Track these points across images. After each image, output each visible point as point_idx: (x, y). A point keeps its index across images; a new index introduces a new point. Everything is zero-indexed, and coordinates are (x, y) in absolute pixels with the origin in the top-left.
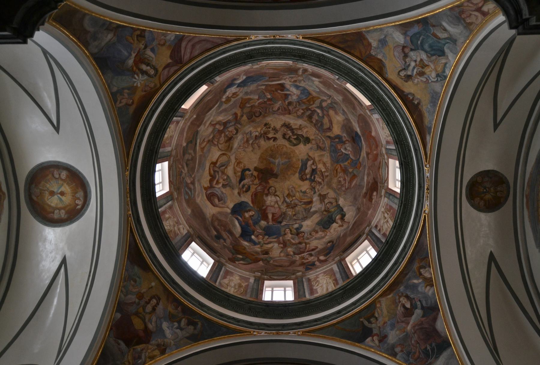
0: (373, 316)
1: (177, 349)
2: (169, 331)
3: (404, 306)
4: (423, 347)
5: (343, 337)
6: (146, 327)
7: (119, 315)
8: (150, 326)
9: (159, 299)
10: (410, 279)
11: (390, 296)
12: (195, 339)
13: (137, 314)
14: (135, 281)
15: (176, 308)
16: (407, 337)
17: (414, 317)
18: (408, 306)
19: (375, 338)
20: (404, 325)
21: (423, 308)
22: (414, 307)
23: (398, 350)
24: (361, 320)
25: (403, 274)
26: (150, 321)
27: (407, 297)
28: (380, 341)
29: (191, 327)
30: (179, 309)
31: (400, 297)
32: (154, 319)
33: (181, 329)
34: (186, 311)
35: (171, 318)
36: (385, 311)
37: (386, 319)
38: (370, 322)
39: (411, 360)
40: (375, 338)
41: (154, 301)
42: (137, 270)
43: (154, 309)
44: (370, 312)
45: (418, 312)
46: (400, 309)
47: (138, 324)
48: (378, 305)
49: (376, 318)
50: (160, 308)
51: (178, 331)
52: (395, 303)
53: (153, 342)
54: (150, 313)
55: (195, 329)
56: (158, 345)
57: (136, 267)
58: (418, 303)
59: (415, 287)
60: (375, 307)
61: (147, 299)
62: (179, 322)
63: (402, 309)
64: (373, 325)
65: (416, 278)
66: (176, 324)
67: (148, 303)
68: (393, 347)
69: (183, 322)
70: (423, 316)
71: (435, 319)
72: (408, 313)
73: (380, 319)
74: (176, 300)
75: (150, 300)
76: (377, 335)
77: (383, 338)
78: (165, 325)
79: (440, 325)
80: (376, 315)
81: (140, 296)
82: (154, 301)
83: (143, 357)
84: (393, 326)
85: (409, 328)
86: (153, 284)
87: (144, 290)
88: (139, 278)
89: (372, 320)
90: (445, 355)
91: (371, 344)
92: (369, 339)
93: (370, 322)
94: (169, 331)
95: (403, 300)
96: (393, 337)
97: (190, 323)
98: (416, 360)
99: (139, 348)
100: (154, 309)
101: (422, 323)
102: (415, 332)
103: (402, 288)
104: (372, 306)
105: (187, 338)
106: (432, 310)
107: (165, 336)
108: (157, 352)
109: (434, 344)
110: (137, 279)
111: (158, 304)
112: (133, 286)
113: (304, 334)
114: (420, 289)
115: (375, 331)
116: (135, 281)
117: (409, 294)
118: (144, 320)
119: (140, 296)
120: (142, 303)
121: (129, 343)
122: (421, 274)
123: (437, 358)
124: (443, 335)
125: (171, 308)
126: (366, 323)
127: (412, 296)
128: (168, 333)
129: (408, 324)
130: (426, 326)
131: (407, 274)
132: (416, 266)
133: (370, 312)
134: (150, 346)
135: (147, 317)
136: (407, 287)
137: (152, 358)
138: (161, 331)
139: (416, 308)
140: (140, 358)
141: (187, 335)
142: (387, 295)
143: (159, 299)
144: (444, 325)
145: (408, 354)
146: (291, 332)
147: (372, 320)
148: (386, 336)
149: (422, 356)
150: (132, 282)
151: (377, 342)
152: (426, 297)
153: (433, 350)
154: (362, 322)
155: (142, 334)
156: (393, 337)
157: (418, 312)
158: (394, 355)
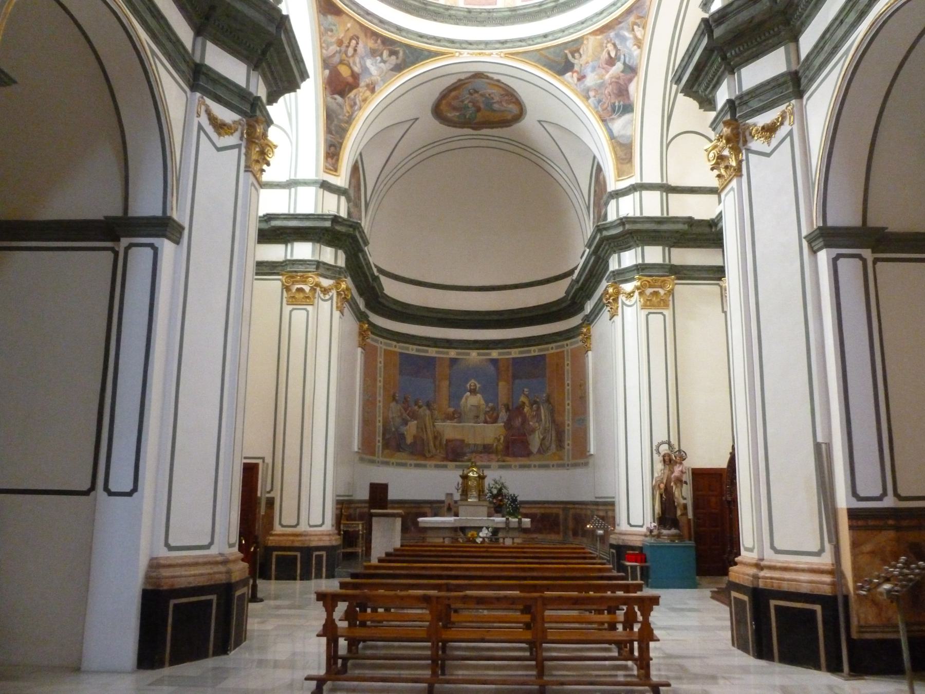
0: (578, 51)
1: (384, 83)
2: (374, 68)
3: (609, 54)
4: (613, 101)
5: (545, 66)
6: (353, 72)
7: (327, 72)
8: (357, 69)
9: (358, 38)
10: (622, 28)
11: (599, 37)
12: (399, 68)
13: (341, 62)
14: (332, 31)
15: (376, 42)
16: (602, 85)
17: (614, 68)
18: (613, 55)
19: (575, 75)
20: (603, 72)
21: (624, 63)
22: (617, 58)
23: (592, 94)
24: (566, 51)
25: (618, 21)
26: (354, 63)
27: (614, 45)
28: (579, 80)
29: (393, 57)
30: (379, 41)
31: (608, 42)
32: (357, 60)
33: (384, 62)
34: (386, 41)
35: (374, 53)
36: (590, 51)
37: (590, 59)
38: (573, 57)
39: (600, 109)
40: (575, 75)
41: (354, 42)
42: (331, 18)
43: (355, 50)
44: (576, 46)
45: (619, 66)
46: (604, 55)
47: (344, 71)
48: (585, 42)
49: (581, 56)
50: (360, 48)
51: (382, 65)
52: (601, 46)
53: (362, 84)
54: (353, 56)
55: (397, 58)
56: (367, 86)
57: (329, 17)
58: (622, 57)
59: (623, 39)
60: (582, 43)
61: (346, 43)
62: (381, 55)
63: (607, 55)
64: (575, 62)
65: (627, 30)
66: (379, 58)
67: (348, 47)
68: (588, 90)
69: (385, 53)
70: (623, 72)
71: (630, 80)
72: (611, 62)
73: (584, 57)
74: (375, 34)
75: (349, 43)
76: (576, 72)
77: (581, 78)
78: (369, 63)
79: (632, 88)
80: (581, 51)
81: (340, 43)
82: (354, 42)
83: (358, 102)
84: (594, 69)
85: (607, 77)
86: (349, 25)
87: (342, 35)
88: (335, 25)
89: (576, 55)
90: (627, 117)
91: (570, 80)
92: (569, 74)
93: (573, 57)
94: (374, 68)
95: (610, 47)
96: (591, 80)
97: (393, 53)
98: (603, 110)
99: (352, 95)
100: (355, 50)
101: (619, 78)
102: (611, 84)
103: (612, 34)
104: (579, 41)
105: (392, 70)
106: (631, 70)
107: (371, 74)
108: (368, 93)
109: (622, 103)
110: (334, 28)
111: (357, 43)
112: (331, 36)
113: (508, 55)
114: (628, 43)
115: (576, 68)
116: (332, 31)
117: (617, 43)
118: (349, 66)
119: (340, 43)
120: (343, 49)
121: (342, 94)
122: (633, 30)
123: (620, 116)
124: (631, 99)
125: (371, 44)
126: (570, 56)
127: (619, 47)
128: (373, 70)
129: (607, 72)
130: (621, 82)
131: (620, 23)
132: (632, 19)
133: (576, 46)
134: (360, 89)
135: (351, 61)
136: (617, 35)
137: (365, 100)
138: (365, 69)
139: (619, 60)
140: (355, 104)
141: (392, 66)
142: (597, 35)
143: (357, 38)
144: (634, 89)
145: (599, 101)
146: (495, 52)
147: (576, 55)
148: (584, 77)
149: (609, 109)
150: (329, 33)
151: (575, 79)
152: (631, 55)
153: (619, 107)
154: (566, 55)
155: (350, 80)
156: (591, 80)
157: (619, 66)
158: (588, 98)
